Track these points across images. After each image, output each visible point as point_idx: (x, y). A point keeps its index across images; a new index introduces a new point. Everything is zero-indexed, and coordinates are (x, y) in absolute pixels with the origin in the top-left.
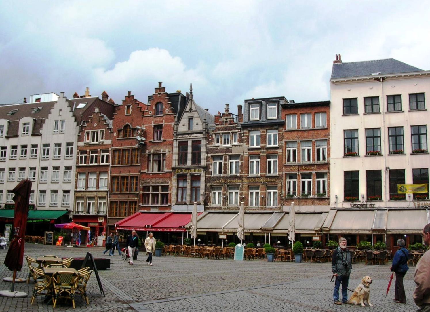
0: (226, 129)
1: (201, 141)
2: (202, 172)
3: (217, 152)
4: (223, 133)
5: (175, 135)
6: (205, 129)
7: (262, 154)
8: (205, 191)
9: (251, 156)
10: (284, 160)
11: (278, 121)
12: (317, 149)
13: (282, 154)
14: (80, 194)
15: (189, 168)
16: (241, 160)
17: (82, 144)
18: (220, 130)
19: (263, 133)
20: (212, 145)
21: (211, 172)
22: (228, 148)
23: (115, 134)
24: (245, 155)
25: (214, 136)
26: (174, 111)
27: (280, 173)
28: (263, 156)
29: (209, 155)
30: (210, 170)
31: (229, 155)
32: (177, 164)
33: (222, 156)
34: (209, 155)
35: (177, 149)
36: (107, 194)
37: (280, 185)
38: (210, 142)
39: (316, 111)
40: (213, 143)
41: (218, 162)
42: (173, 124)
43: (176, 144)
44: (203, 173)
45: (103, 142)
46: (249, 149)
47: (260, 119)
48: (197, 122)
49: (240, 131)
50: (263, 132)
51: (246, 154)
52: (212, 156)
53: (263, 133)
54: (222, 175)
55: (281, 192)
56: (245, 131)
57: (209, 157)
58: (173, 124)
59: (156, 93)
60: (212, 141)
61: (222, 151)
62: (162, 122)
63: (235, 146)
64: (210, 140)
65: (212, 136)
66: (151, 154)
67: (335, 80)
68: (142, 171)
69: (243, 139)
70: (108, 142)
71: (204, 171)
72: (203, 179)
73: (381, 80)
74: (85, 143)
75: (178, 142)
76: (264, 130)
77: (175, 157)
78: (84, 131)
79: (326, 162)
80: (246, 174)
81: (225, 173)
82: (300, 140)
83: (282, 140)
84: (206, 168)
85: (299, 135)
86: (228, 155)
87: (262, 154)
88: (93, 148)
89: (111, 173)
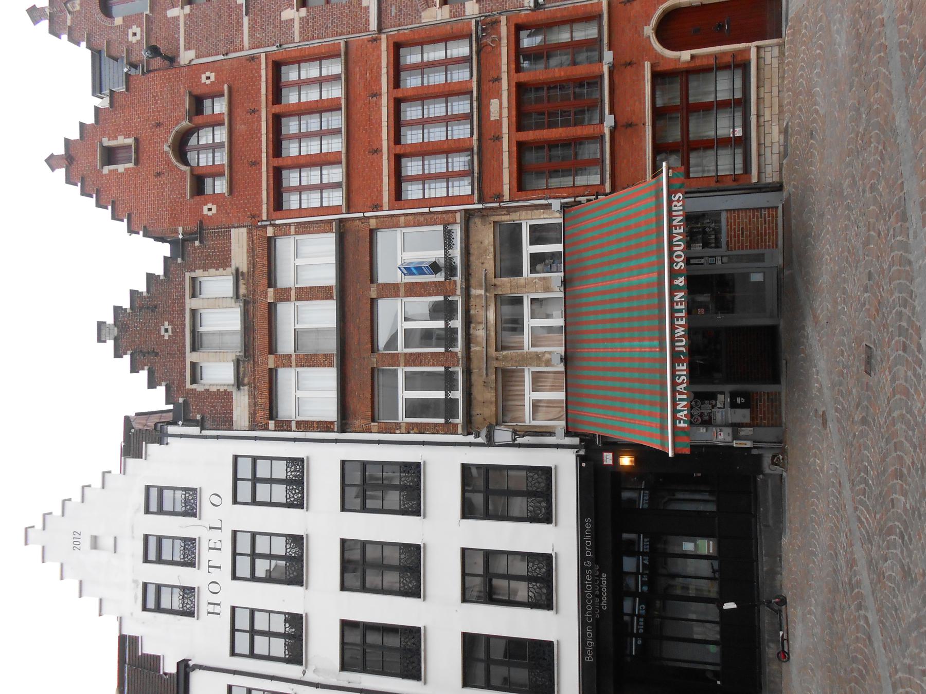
36: (483, 214)
45: (237, 275)
59: (69, 23)
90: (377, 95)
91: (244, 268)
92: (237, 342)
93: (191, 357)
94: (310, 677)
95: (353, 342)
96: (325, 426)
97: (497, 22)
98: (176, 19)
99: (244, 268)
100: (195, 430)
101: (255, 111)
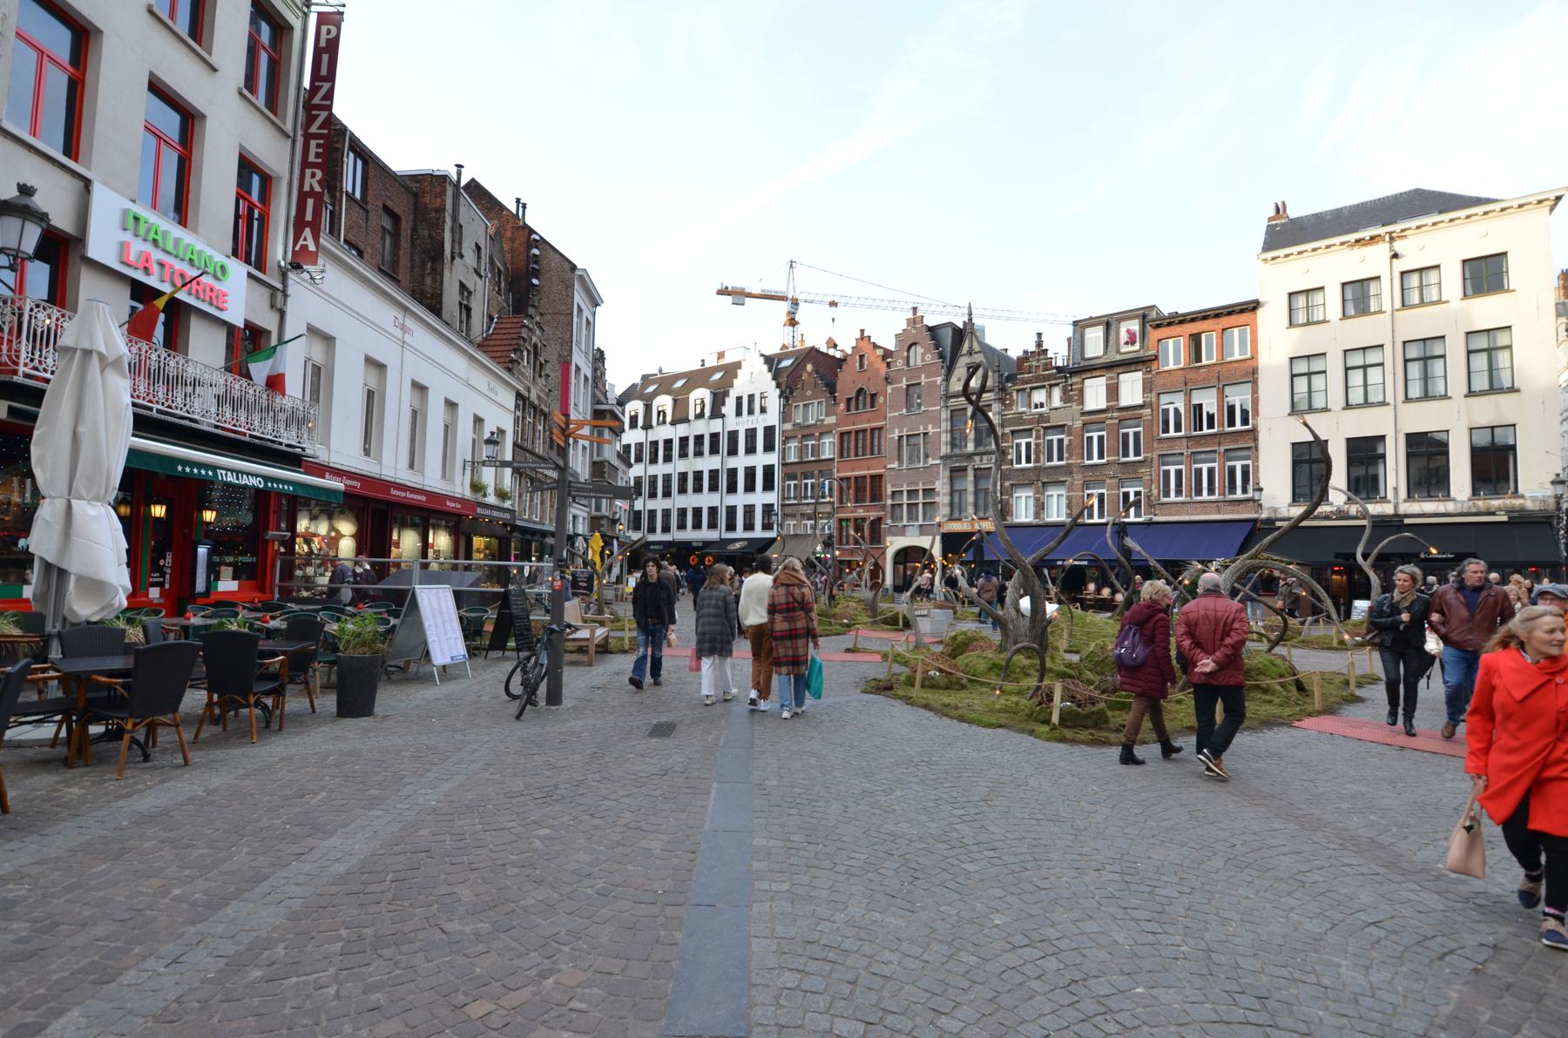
0: (1037, 379)
3: (1021, 424)
4: (1032, 389)
5: (944, 398)
7: (1109, 422)
14: (789, 510)
15: (970, 456)
16: (1068, 436)
17: (788, 426)
18: (1027, 383)
21: (1012, 460)
22: (1041, 415)
23: (842, 406)
25: (1014, 394)
26: (941, 356)
27: (1149, 455)
30: (1009, 457)
31: (1045, 428)
32: (949, 451)
33: (1031, 430)
35: (949, 423)
37: (1149, 478)
38: (1008, 407)
40: (1014, 408)
41: (1023, 442)
43: (945, 415)
45: (823, 420)
50: (1111, 378)
51: (1078, 424)
52: (1013, 432)
54: (1031, 465)
55: (1151, 490)
56: (1075, 380)
57: (1006, 434)
58: (939, 380)
60: (1010, 405)
61: (1030, 422)
62: (920, 378)
65: (1010, 394)
68: (889, 466)
70: (831, 420)
73: (1387, 238)
74: (794, 425)
75: (949, 412)
76: (1112, 375)
77: (945, 438)
79: (1250, 427)
80: (1079, 461)
81: (1037, 460)
82: (1188, 388)
83: (1151, 392)
87: (1109, 422)
88: (806, 432)
89: (838, 471)
90: (869, 469)
92: (807, 423)
93: (801, 404)
95: (803, 466)
96: (784, 458)
97: (883, 510)
98: (901, 382)
101: (869, 421)
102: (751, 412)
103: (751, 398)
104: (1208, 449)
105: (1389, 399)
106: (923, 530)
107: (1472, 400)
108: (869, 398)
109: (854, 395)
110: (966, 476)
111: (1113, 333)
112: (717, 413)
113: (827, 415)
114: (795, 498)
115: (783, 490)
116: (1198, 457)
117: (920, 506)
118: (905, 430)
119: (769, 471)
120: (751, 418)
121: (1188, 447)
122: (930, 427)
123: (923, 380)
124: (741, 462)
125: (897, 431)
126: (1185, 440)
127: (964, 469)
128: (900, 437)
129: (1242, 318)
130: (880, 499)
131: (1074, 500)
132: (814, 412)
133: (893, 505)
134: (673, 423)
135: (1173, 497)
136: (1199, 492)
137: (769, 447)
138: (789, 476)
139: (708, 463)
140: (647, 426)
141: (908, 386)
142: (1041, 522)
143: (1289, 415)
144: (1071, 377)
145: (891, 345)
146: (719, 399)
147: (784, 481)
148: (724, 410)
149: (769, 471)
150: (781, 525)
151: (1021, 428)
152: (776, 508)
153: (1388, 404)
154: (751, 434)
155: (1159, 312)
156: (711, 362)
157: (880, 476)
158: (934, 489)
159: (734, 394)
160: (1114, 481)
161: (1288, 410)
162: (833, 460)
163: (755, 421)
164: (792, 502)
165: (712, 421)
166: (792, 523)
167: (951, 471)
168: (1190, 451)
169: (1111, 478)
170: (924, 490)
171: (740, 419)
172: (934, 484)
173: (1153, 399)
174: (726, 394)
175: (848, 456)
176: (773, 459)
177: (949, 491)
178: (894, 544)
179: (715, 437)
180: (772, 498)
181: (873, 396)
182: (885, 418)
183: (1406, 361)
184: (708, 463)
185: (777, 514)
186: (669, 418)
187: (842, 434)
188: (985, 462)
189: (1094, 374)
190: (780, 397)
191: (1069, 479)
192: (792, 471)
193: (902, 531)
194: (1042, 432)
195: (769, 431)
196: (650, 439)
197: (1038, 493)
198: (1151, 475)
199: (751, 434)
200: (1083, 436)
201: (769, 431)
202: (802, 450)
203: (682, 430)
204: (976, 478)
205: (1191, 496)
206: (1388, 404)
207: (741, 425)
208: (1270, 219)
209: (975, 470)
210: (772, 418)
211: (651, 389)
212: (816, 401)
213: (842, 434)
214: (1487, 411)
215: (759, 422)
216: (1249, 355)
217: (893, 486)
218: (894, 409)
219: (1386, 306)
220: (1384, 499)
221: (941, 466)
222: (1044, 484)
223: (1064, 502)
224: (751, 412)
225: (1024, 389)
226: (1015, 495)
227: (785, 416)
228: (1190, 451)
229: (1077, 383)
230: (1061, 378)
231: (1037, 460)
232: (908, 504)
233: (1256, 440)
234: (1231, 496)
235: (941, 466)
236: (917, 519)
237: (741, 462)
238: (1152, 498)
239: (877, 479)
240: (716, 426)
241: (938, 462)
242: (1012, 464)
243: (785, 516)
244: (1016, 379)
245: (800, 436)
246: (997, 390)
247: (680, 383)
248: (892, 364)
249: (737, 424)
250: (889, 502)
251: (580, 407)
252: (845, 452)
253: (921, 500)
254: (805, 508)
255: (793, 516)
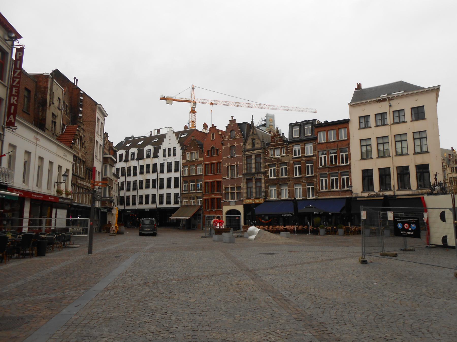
0: (277, 145)
1: (261, 154)
2: (262, 176)
4: (275, 148)
5: (244, 151)
6: (262, 147)
7: (302, 161)
8: (265, 189)
9: (295, 163)
10: (317, 164)
11: (312, 137)
12: (341, 155)
13: (316, 160)
14: (185, 196)
15: (253, 174)
16: (288, 166)
17: (184, 161)
19: (302, 147)
20: (268, 157)
21: (269, 175)
22: (278, 158)
23: (205, 154)
24: (290, 163)
25: (269, 150)
26: (243, 135)
27: (315, 174)
28: (303, 162)
29: (267, 164)
30: (268, 174)
31: (280, 163)
32: (246, 172)
33: (275, 164)
34: (267, 164)
35: (246, 161)
36: (202, 194)
37: (316, 182)
38: (267, 155)
39: (340, 128)
41: (273, 168)
42: (242, 144)
44: (263, 177)
45: (198, 159)
46: (293, 158)
47: (300, 136)
48: (257, 142)
49: (287, 146)
50: (302, 145)
51: (292, 162)
52: (269, 165)
53: (302, 147)
54: (275, 177)
55: (317, 187)
56: (290, 146)
57: (266, 165)
58: (242, 144)
61: (275, 161)
62: (235, 143)
63: (284, 156)
64: (267, 153)
65: (268, 150)
66: (229, 166)
67: (352, 104)
68: (224, 178)
69: (289, 151)
70: (201, 159)
71: (263, 175)
72: (263, 181)
73: (388, 100)
78: (186, 152)
79: (348, 164)
80: (292, 176)
81: (278, 176)
82: (328, 150)
84: (265, 173)
85: (328, 146)
86: (279, 163)
87: (302, 161)
91: (199, 160)
94: (159, 174)
97: (222, 195)
98: (228, 145)
99: (199, 160)
100: (182, 155)
101: (216, 160)
102: (169, 155)
103: (170, 149)
104: (335, 172)
105: (391, 155)
106: (237, 203)
107: (416, 156)
108: (215, 151)
109: (210, 149)
110: (252, 182)
111: (302, 129)
112: (155, 156)
113: (200, 157)
114: (187, 191)
115: (182, 187)
116: (333, 175)
117: (236, 193)
118: (229, 163)
119: (176, 179)
120: (169, 158)
121: (328, 171)
122: (239, 162)
123: (236, 144)
124: (165, 176)
125: (226, 164)
126: (327, 169)
127: (251, 179)
128: (228, 166)
129: (344, 125)
130: (220, 191)
131: (291, 191)
132: (194, 156)
133: (225, 193)
134: (137, 159)
135: (324, 190)
136: (333, 188)
137: (177, 170)
138: (185, 182)
139: (151, 176)
140: (126, 161)
141: (230, 146)
142: (279, 199)
143: (360, 160)
144: (289, 144)
145: (224, 129)
146: (156, 150)
147: (183, 184)
148: (158, 154)
149: (176, 179)
150: (182, 202)
151: (272, 163)
152: (179, 195)
153: (390, 157)
154: (169, 165)
155: (318, 121)
156: (155, 134)
157: (220, 182)
158: (241, 187)
159: (162, 148)
160: (304, 183)
161: (360, 158)
162: (202, 175)
163: (171, 159)
164: (186, 192)
165: (154, 159)
166: (186, 201)
167: (247, 180)
168: (329, 172)
169: (303, 182)
170: (237, 187)
171: (165, 158)
172: (240, 185)
173: (316, 153)
174: (160, 148)
175: (208, 174)
176: (178, 174)
177: (246, 187)
178: (226, 209)
179: (155, 165)
180: (178, 190)
181: (217, 150)
182: (222, 159)
183: (396, 142)
184: (151, 176)
185: (180, 197)
186: (136, 157)
187: (205, 165)
188: (259, 176)
189: (298, 144)
190: (181, 149)
191: (289, 183)
192: (186, 179)
193: (229, 204)
194: (279, 165)
195: (177, 163)
196: (128, 166)
197: (278, 188)
198: (317, 181)
199: (169, 165)
200: (293, 166)
201: (177, 163)
202: (190, 171)
203: (141, 162)
204: (256, 182)
205: (330, 189)
206: (390, 157)
207: (165, 161)
208: (356, 89)
209: (255, 179)
210: (178, 157)
211: (128, 145)
212: (195, 152)
213: (205, 165)
214: (421, 160)
215: (173, 160)
216: (347, 138)
217: (225, 186)
218: (225, 155)
219: (389, 123)
220: (390, 190)
221: (243, 178)
222: (280, 185)
223: (287, 191)
224: (169, 155)
225: (272, 149)
226: (270, 189)
227: (183, 157)
228: (329, 172)
229: (290, 147)
230: (285, 145)
231: (278, 176)
232: (231, 193)
233: (350, 169)
234: (343, 189)
235: (243, 178)
236: (234, 199)
237: (165, 176)
238: (318, 190)
239: (219, 183)
240: (155, 161)
241: (242, 176)
242: (269, 177)
243: (183, 198)
244: (270, 145)
245: (189, 166)
246: (262, 149)
247: (140, 143)
248: (224, 138)
249: (164, 160)
250: (224, 192)
251: (98, 154)
252: (207, 172)
253: (236, 191)
254: (191, 195)
255: (186, 198)
